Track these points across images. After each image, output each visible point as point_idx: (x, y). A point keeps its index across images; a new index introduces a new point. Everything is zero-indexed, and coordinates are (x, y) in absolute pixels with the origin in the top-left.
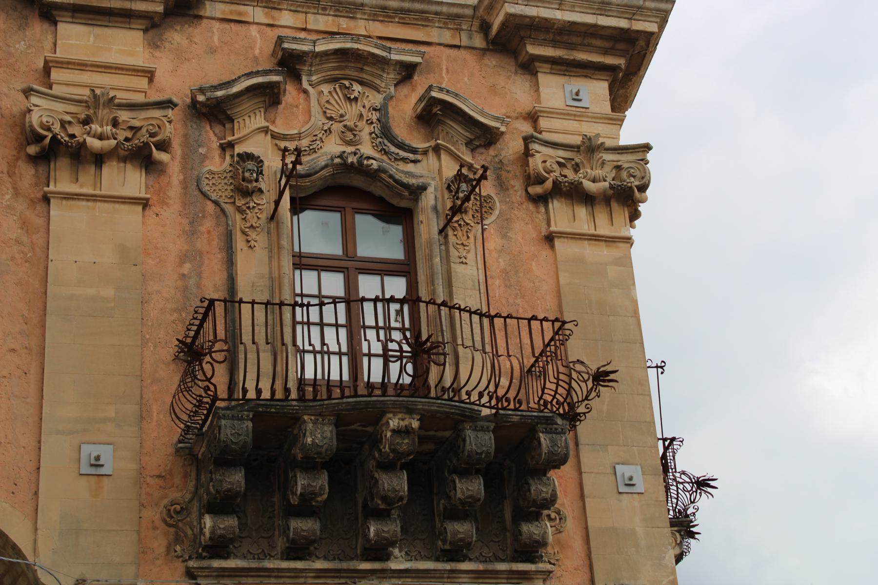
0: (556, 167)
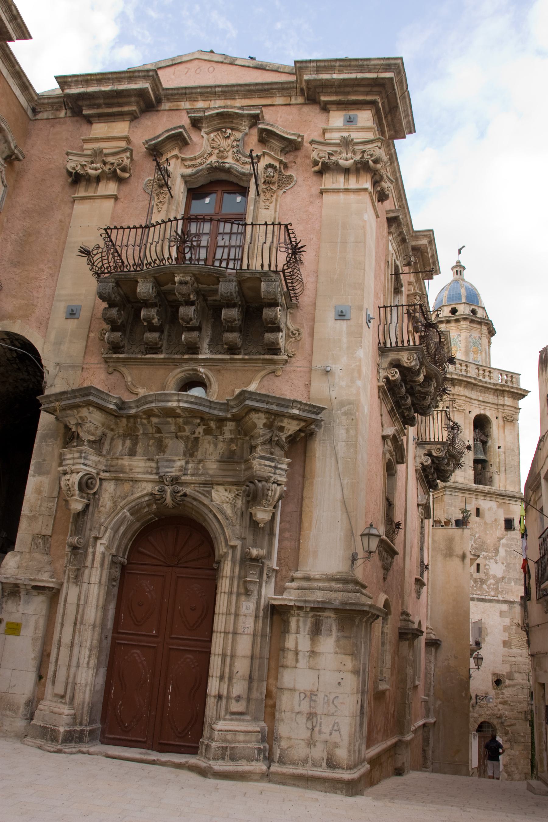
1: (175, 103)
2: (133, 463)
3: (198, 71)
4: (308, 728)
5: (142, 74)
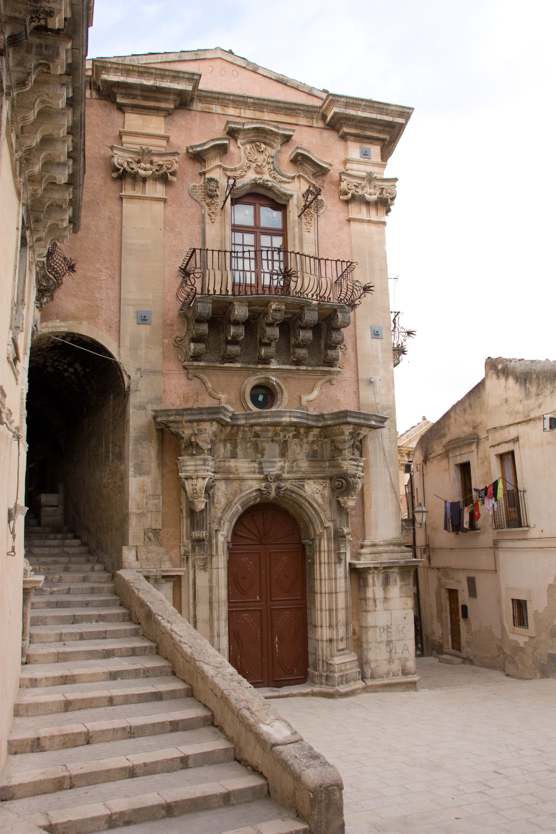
0: (353, 187)
1: (207, 105)
2: (238, 464)
3: (223, 73)
4: (387, 652)
5: (187, 76)
